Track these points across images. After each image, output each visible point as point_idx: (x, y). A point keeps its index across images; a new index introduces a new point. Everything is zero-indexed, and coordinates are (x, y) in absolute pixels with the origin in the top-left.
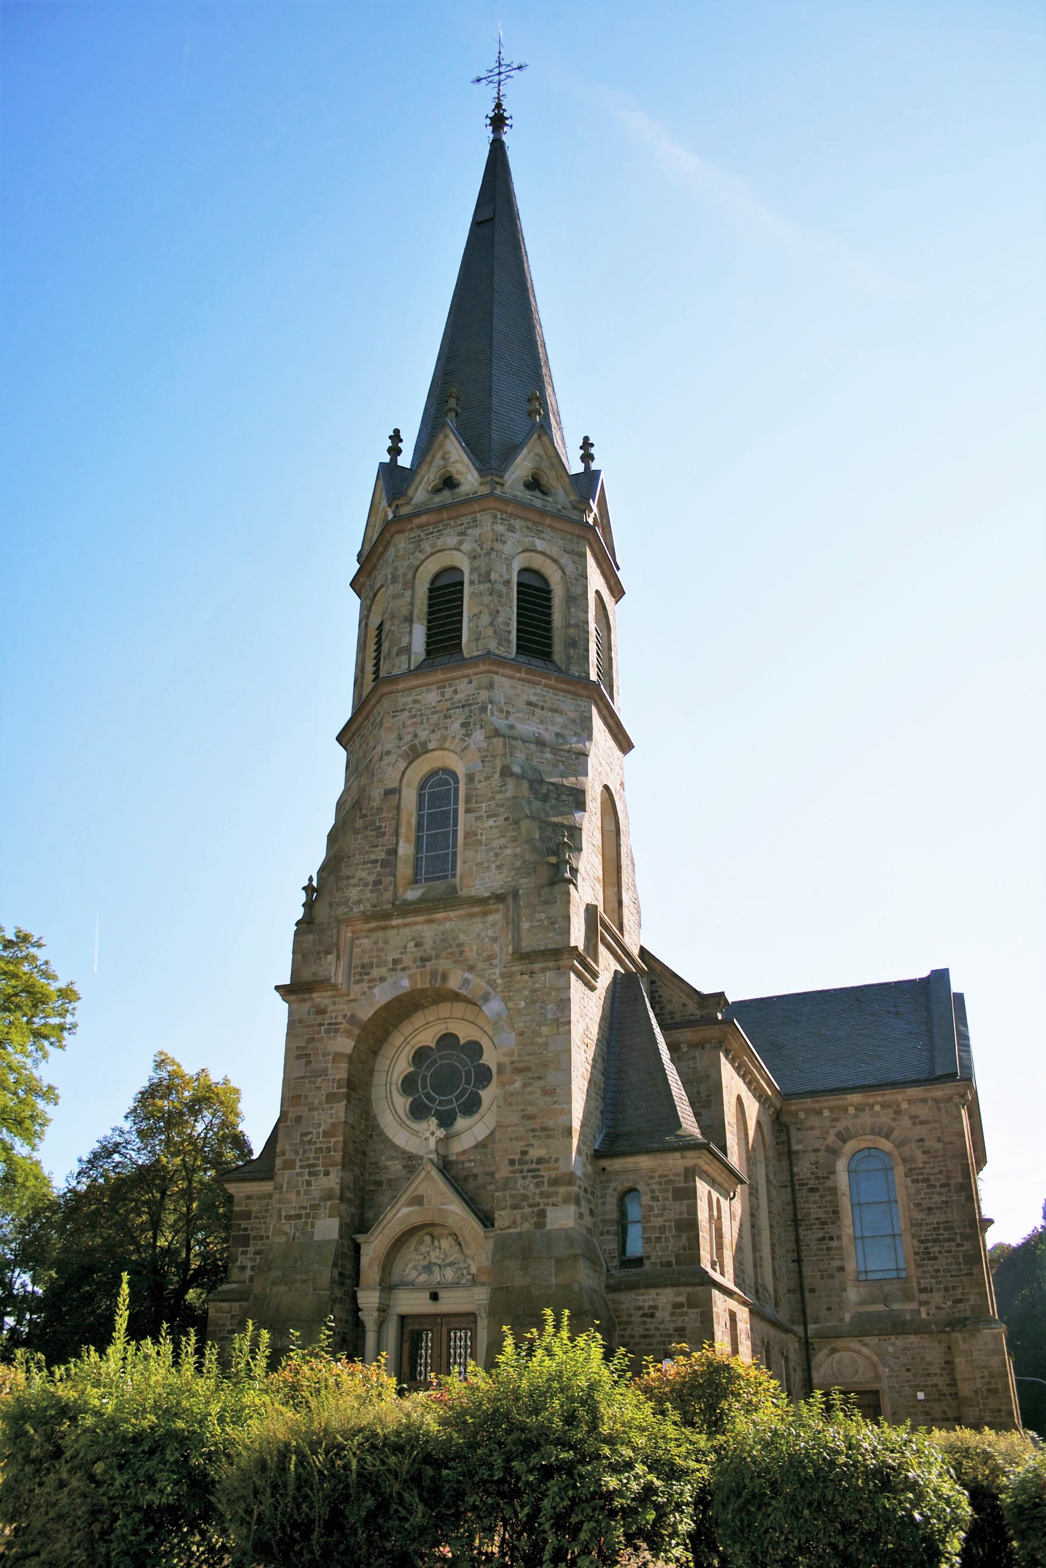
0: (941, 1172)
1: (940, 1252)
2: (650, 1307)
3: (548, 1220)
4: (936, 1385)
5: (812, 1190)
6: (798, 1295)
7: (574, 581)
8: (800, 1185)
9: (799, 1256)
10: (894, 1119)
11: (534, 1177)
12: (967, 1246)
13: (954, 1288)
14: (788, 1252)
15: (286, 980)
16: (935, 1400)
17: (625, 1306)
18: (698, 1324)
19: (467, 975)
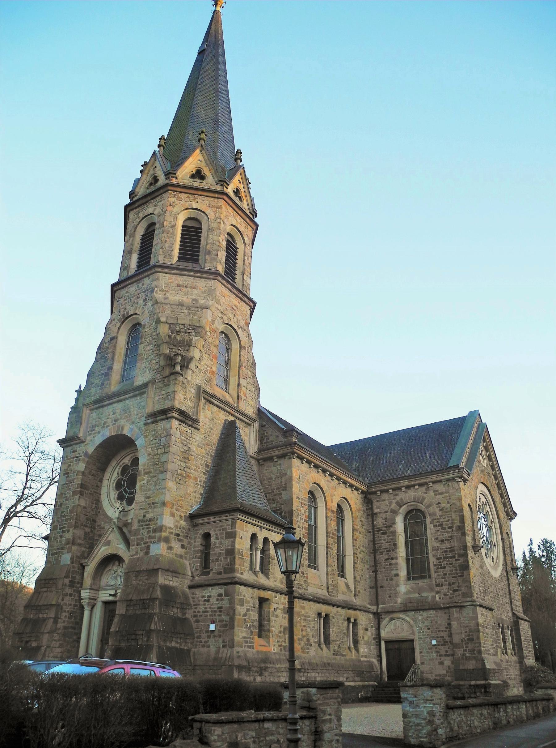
0: (449, 520)
1: (447, 564)
2: (208, 596)
3: (151, 551)
4: (443, 637)
5: (384, 533)
6: (375, 590)
7: (213, 221)
8: (377, 531)
9: (376, 569)
10: (425, 493)
11: (147, 528)
12: (462, 560)
13: (454, 583)
14: (370, 567)
15: (63, 436)
16: (442, 645)
17: (197, 596)
18: (228, 605)
19: (132, 426)
